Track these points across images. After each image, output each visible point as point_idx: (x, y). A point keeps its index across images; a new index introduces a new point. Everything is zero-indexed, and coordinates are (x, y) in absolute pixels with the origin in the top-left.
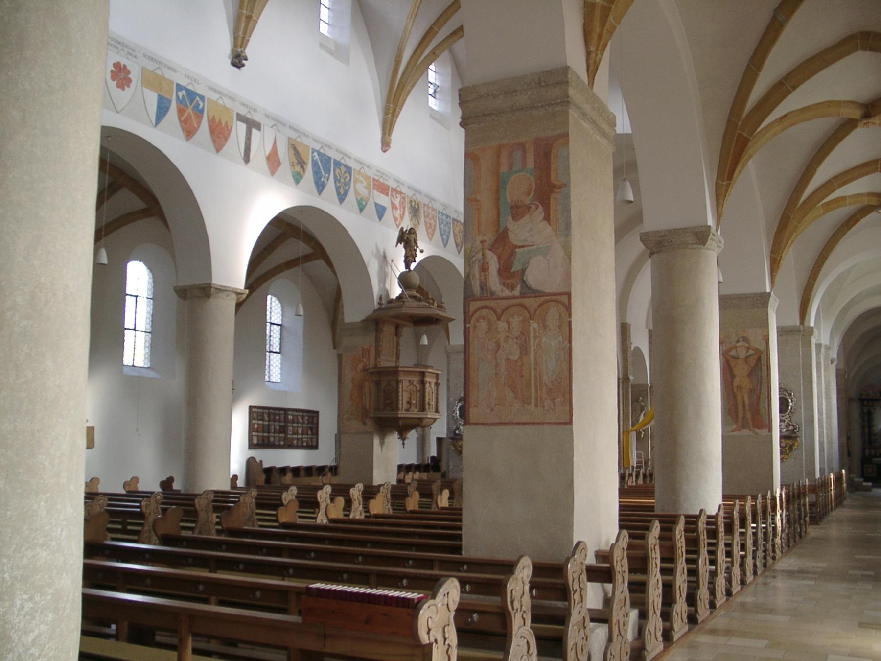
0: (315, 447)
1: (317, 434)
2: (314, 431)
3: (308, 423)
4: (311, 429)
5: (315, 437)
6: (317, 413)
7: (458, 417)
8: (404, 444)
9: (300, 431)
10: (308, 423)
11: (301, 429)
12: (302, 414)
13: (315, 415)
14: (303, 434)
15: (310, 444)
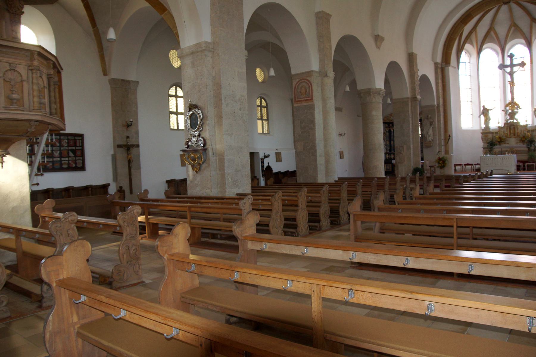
0: (82, 168)
1: (83, 155)
2: (79, 153)
3: (68, 146)
4: (74, 152)
5: (81, 158)
6: (82, 136)
7: (190, 128)
8: (268, 164)
9: (57, 154)
10: (68, 146)
11: (59, 152)
12: (66, 137)
13: (80, 138)
14: (61, 156)
15: (74, 165)
